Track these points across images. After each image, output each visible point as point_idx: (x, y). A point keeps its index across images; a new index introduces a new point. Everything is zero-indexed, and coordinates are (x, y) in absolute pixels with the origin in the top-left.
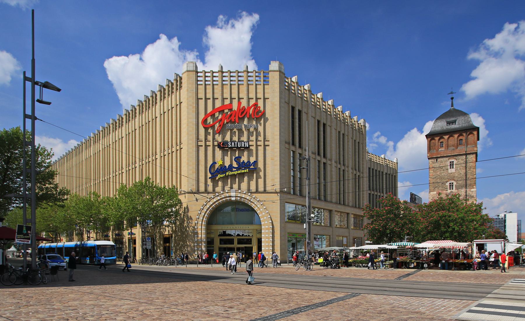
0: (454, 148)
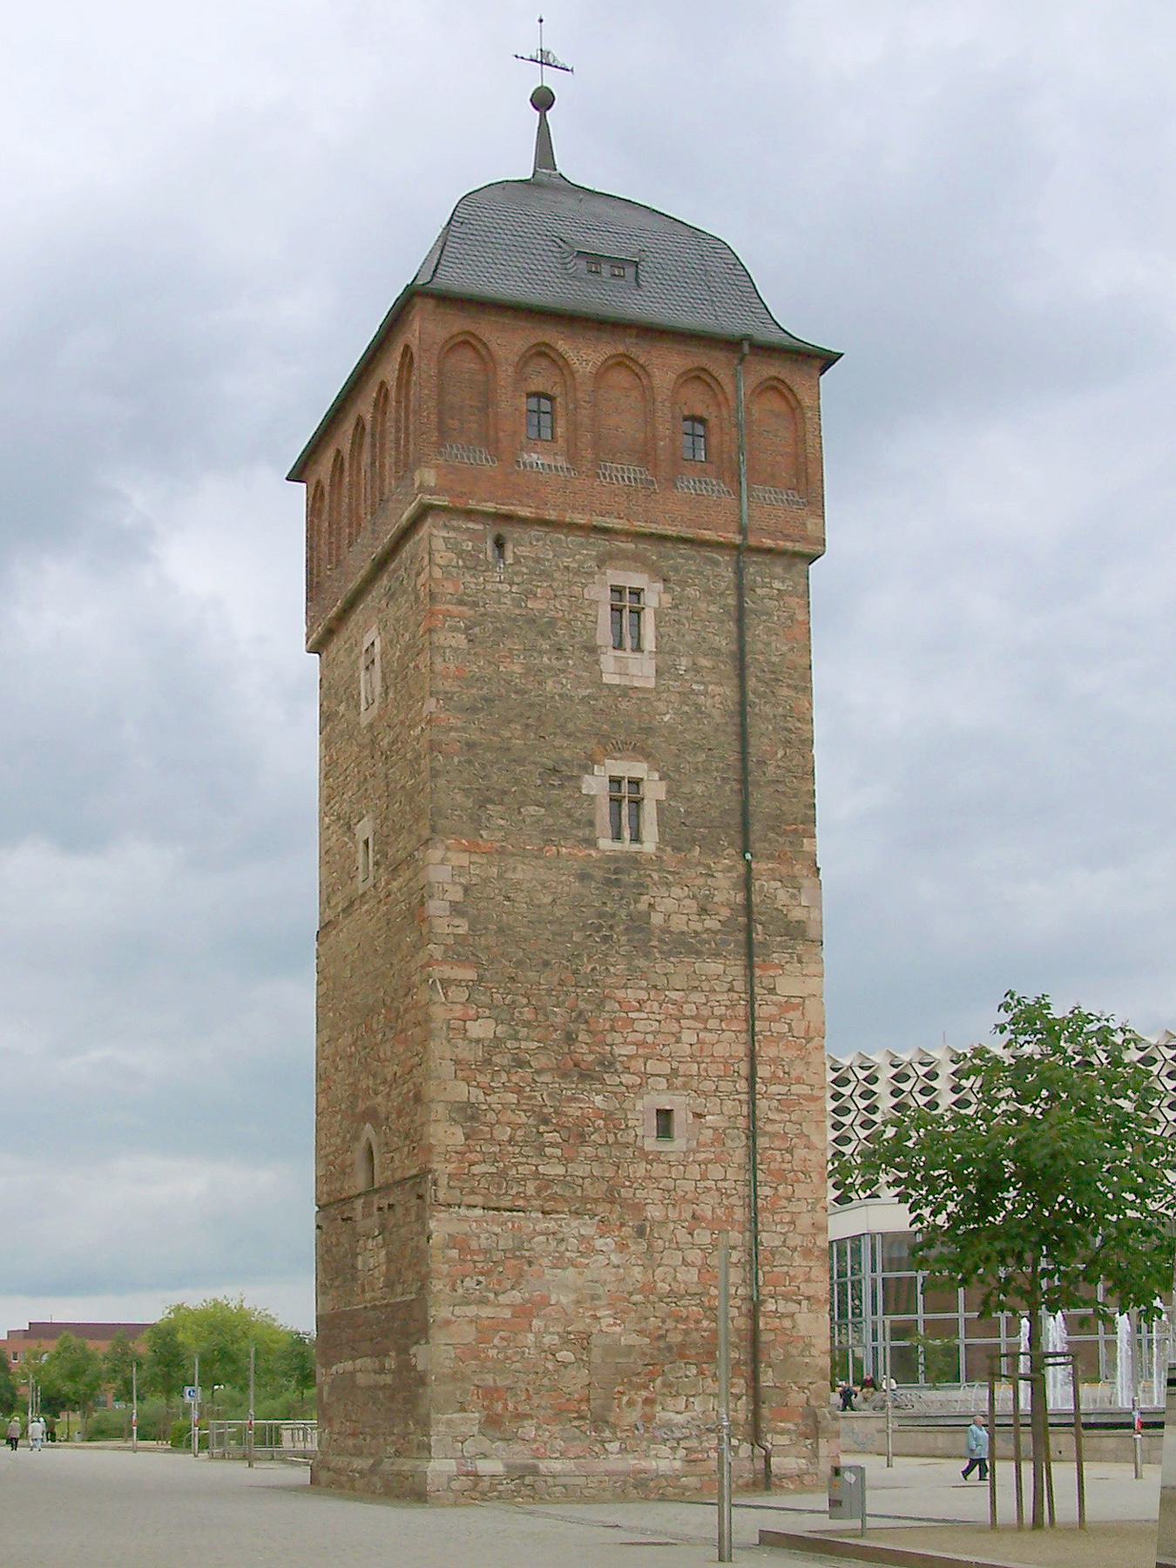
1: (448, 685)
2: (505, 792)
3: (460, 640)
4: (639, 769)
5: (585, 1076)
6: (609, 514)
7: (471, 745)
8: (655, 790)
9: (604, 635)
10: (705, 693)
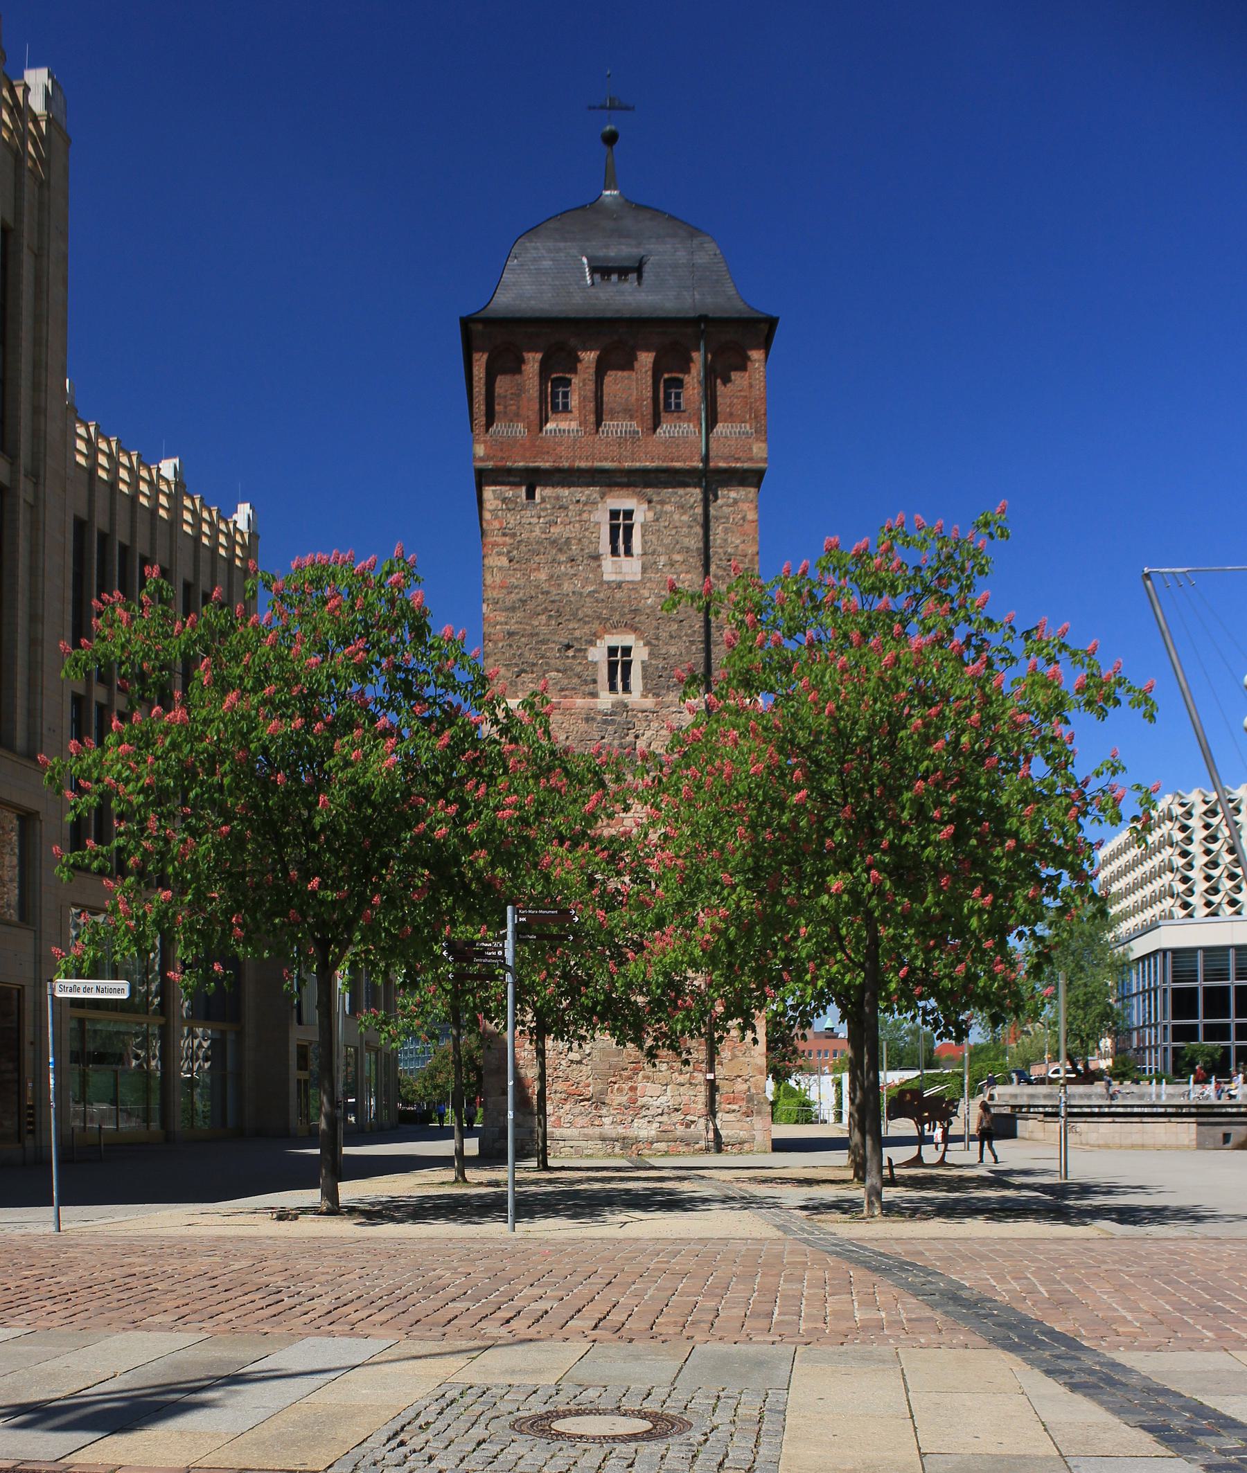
2: (534, 665)
4: (627, 639)
7: (511, 634)
8: (640, 654)
9: (605, 546)
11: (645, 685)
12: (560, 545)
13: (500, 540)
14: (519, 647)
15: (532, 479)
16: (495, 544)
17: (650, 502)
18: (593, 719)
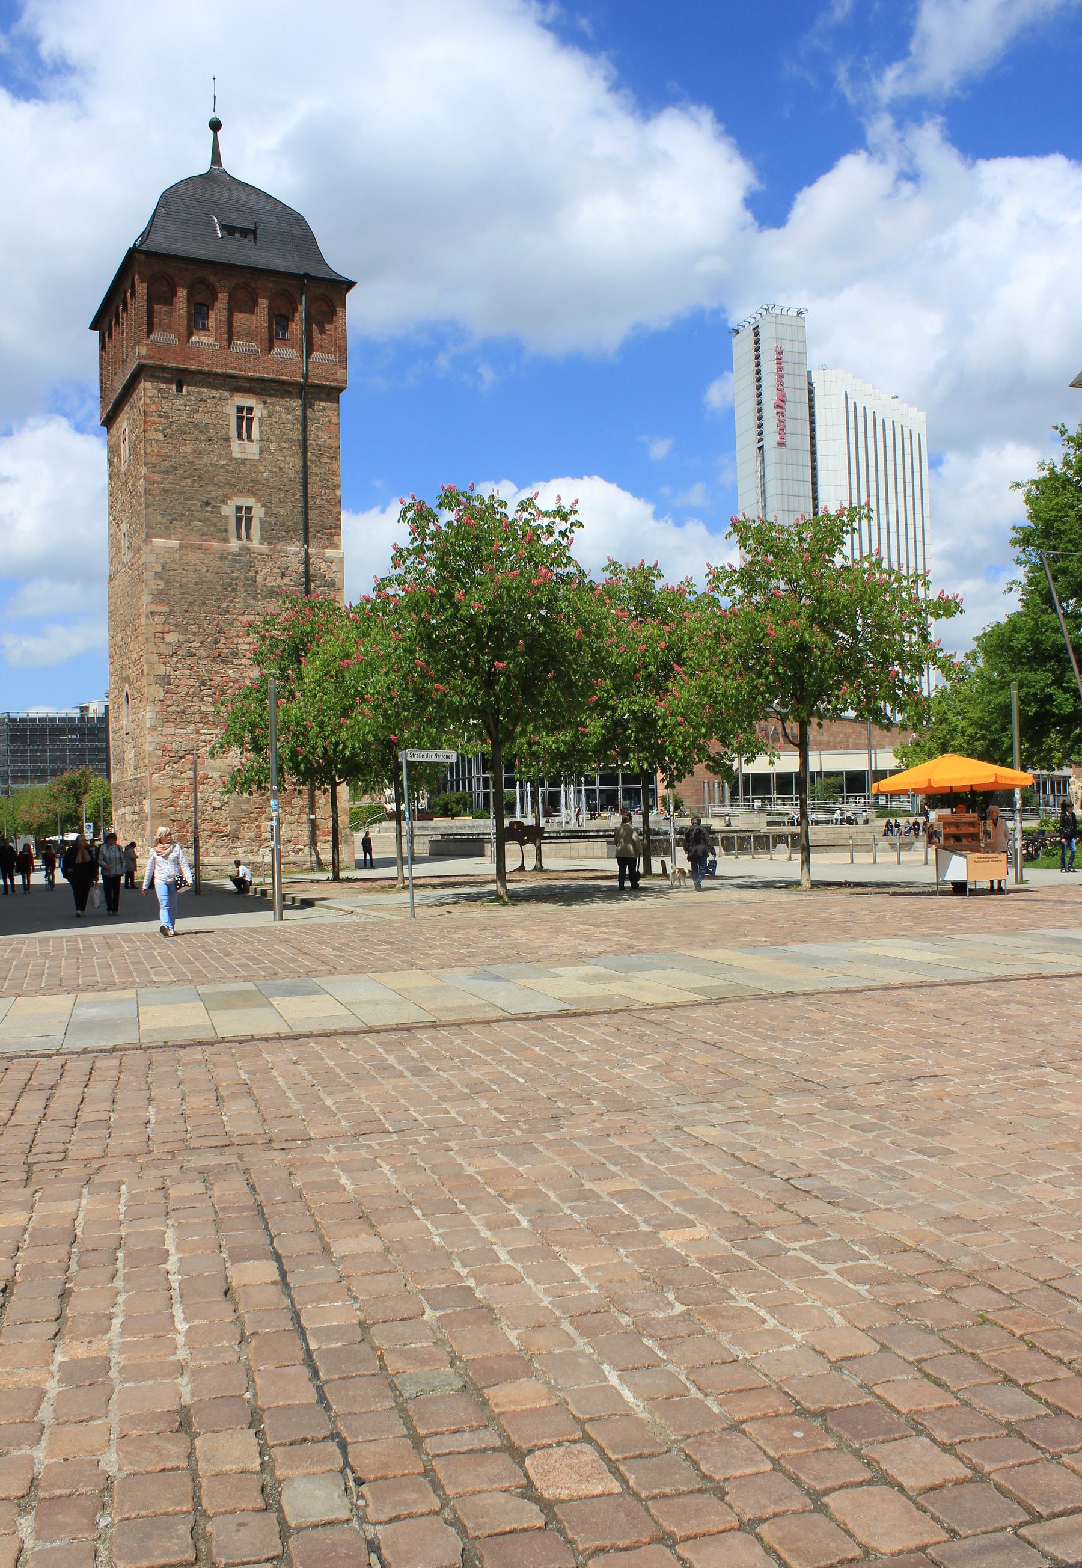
0: (254, 346)
1: (154, 460)
2: (183, 515)
3: (160, 436)
4: (250, 501)
5: (225, 661)
6: (236, 369)
7: (165, 491)
8: (258, 513)
9: (233, 432)
10: (285, 461)
11: (262, 536)
12: (203, 428)
13: (157, 419)
14: (171, 502)
15: (181, 378)
16: (153, 423)
17: (265, 403)
18: (226, 558)
